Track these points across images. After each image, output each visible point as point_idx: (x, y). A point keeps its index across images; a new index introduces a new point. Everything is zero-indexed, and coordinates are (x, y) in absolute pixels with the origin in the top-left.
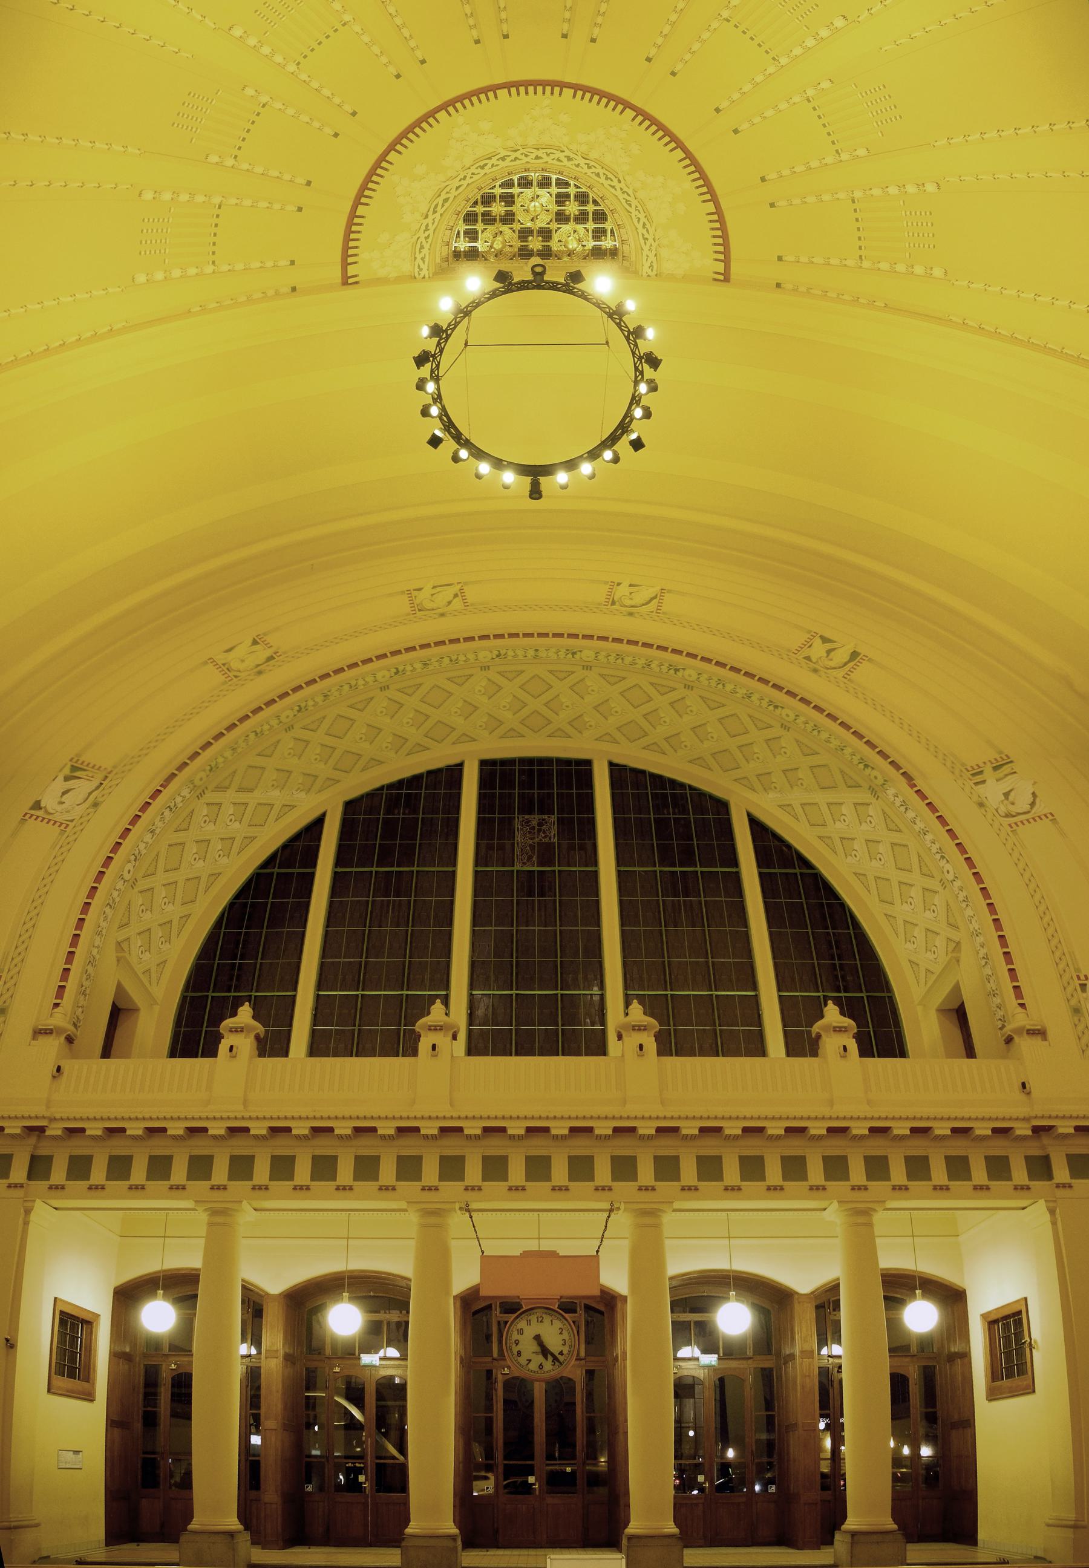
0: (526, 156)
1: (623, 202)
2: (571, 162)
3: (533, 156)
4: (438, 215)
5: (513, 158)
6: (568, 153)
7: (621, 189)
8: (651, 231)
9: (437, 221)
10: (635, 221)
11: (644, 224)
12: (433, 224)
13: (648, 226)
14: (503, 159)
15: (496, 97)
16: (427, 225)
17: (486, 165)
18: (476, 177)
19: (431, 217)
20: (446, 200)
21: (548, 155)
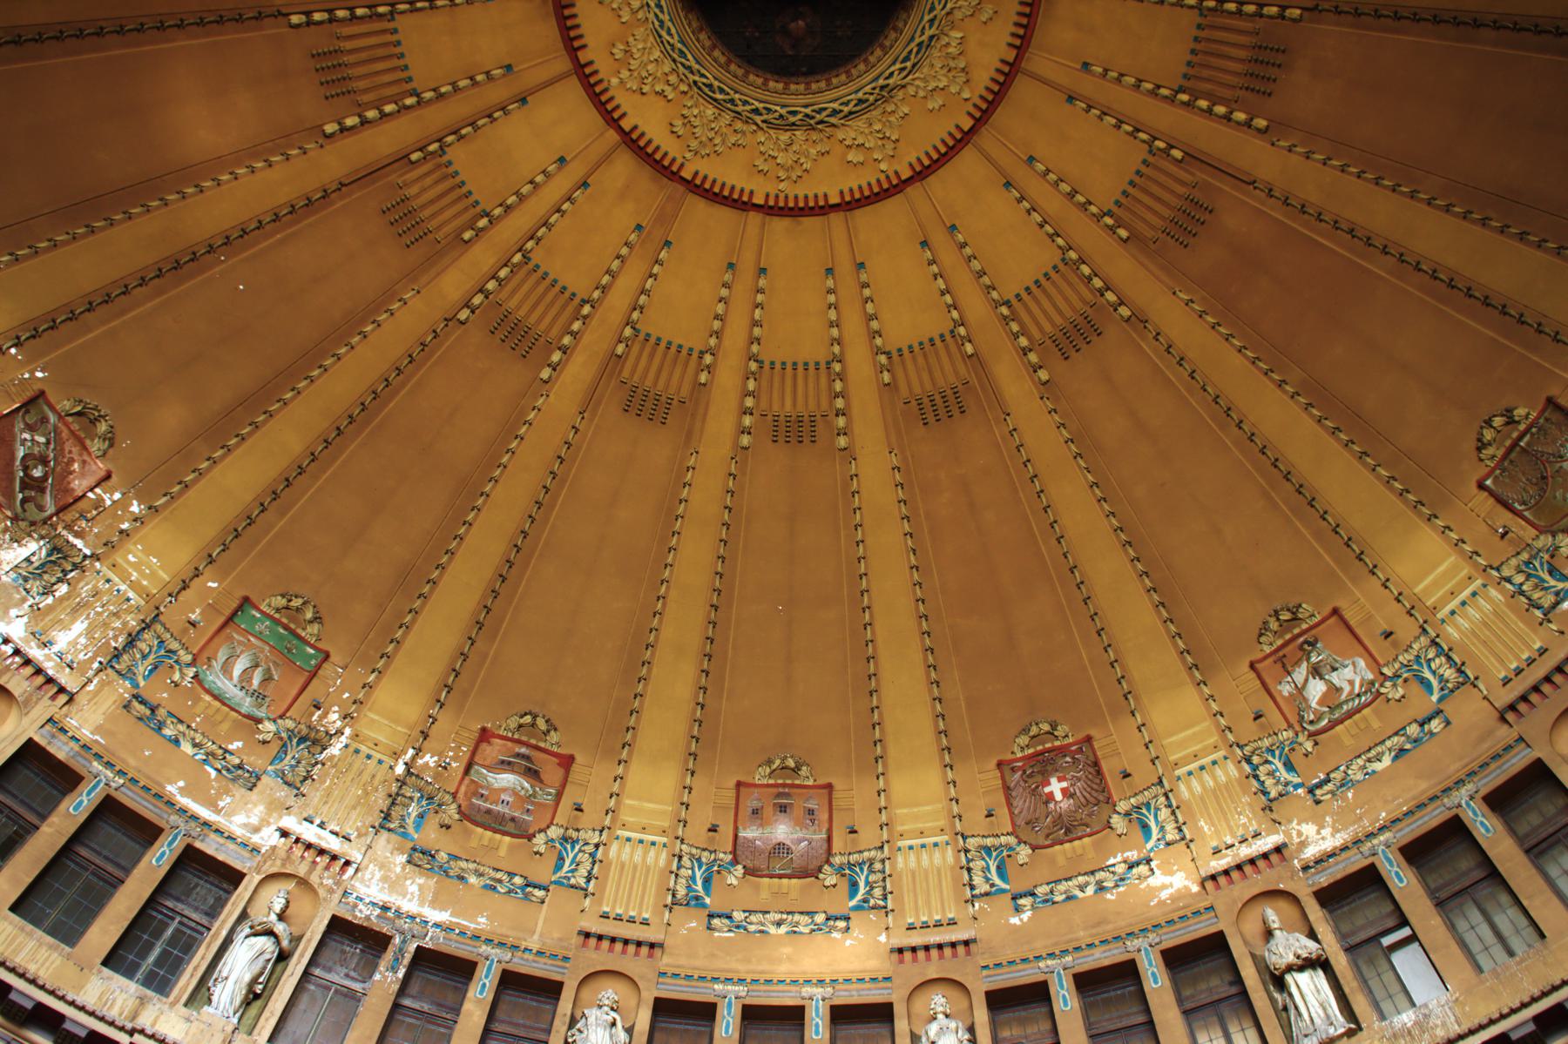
0: (807, 116)
1: (689, 56)
2: (753, 107)
3: (800, 116)
4: (917, 40)
5: (824, 114)
6: (758, 119)
7: (692, 73)
8: (651, 16)
9: (918, 33)
10: (673, 31)
11: (662, 26)
12: (924, 28)
13: (657, 23)
14: (835, 112)
15: (842, 193)
16: (930, 27)
17: (855, 105)
18: (868, 89)
19: (924, 38)
20: (906, 59)
21: (781, 116)
